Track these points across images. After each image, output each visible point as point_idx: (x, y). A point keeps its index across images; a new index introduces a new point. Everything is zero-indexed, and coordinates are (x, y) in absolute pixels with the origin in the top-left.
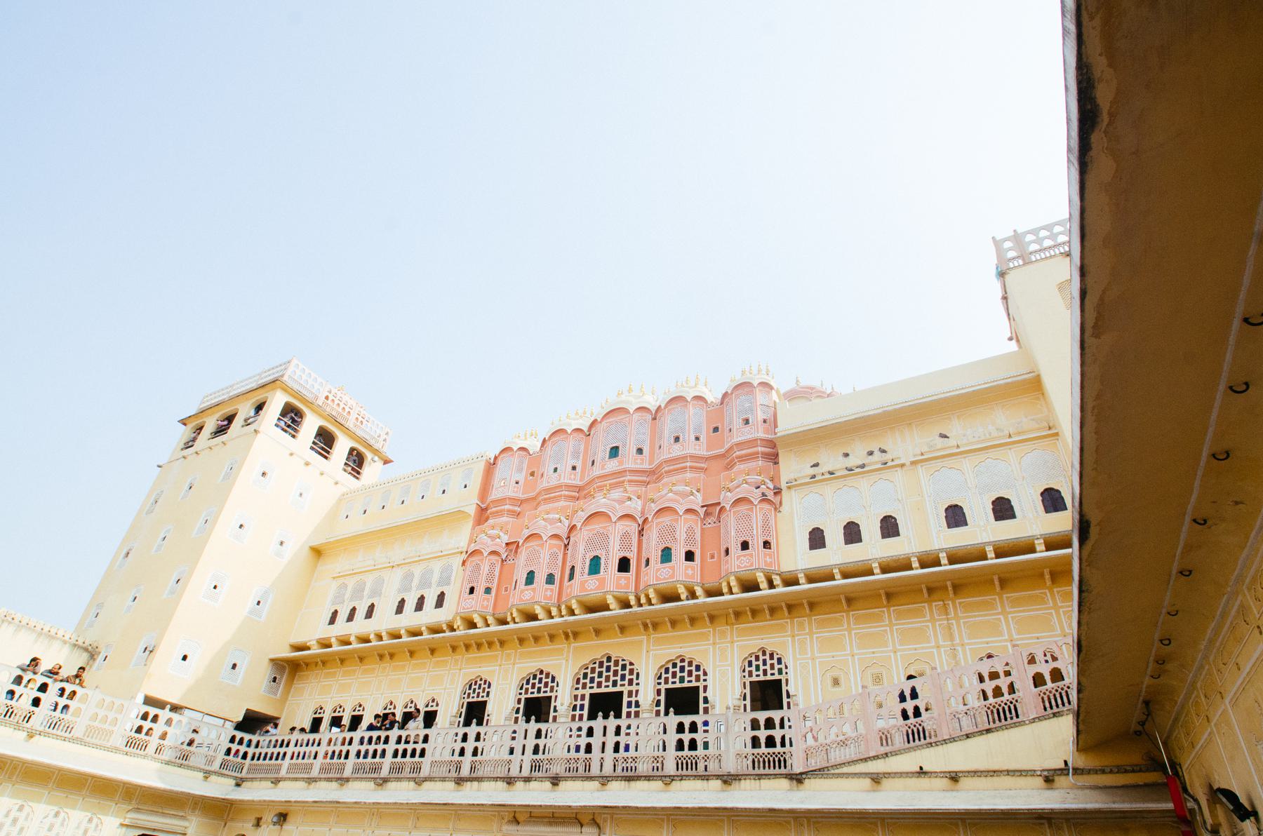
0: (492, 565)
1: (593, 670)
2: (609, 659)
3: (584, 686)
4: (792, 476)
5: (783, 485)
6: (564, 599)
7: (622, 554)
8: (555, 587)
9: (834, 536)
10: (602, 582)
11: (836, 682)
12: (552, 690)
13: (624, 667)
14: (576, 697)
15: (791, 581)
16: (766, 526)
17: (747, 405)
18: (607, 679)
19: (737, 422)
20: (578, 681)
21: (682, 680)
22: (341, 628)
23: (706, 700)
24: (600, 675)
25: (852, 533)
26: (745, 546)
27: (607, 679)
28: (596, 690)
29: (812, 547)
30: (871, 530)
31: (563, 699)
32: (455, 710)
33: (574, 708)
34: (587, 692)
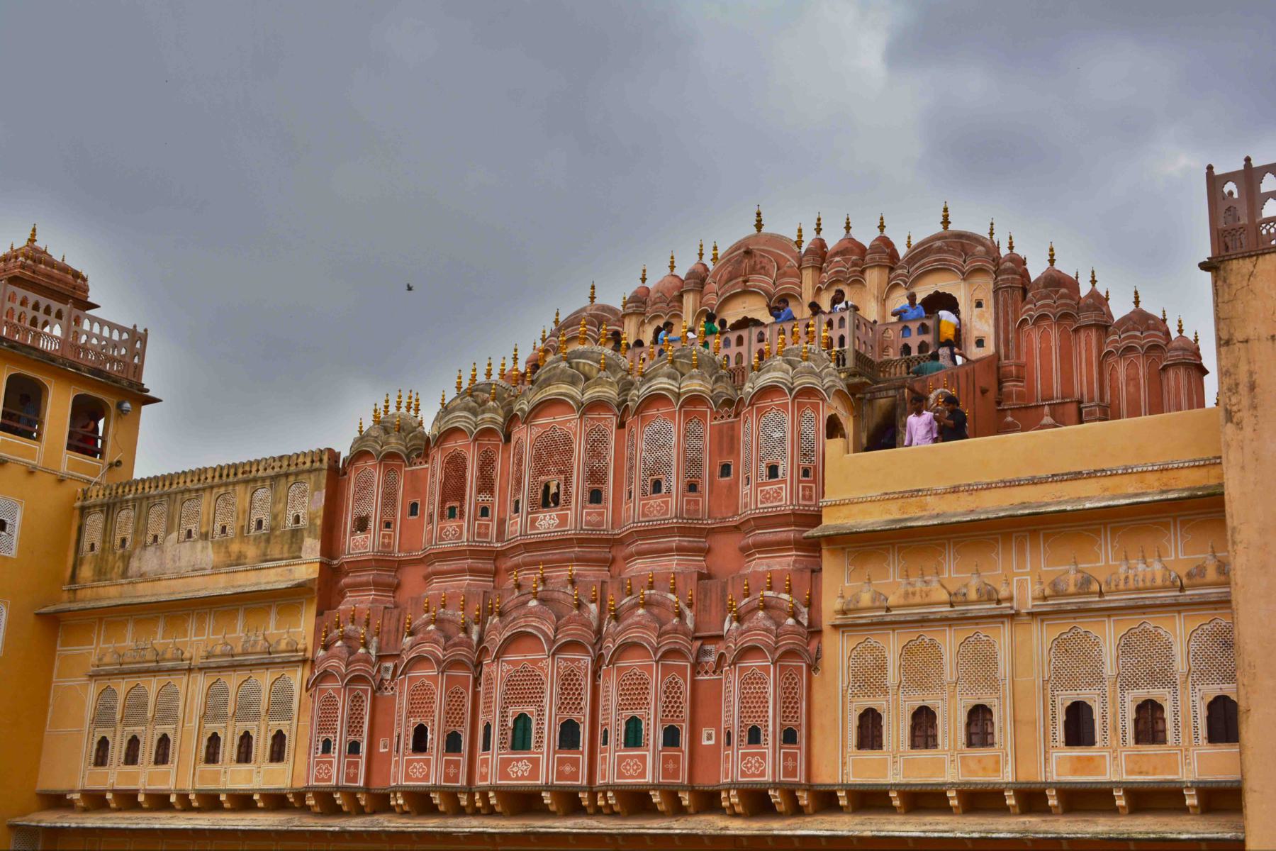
0: (357, 699)
4: (838, 604)
7: (566, 716)
8: (463, 760)
9: (896, 729)
10: (535, 762)
15: (826, 801)
16: (788, 703)
17: (776, 435)
26: (754, 736)
29: (861, 745)
30: (952, 725)
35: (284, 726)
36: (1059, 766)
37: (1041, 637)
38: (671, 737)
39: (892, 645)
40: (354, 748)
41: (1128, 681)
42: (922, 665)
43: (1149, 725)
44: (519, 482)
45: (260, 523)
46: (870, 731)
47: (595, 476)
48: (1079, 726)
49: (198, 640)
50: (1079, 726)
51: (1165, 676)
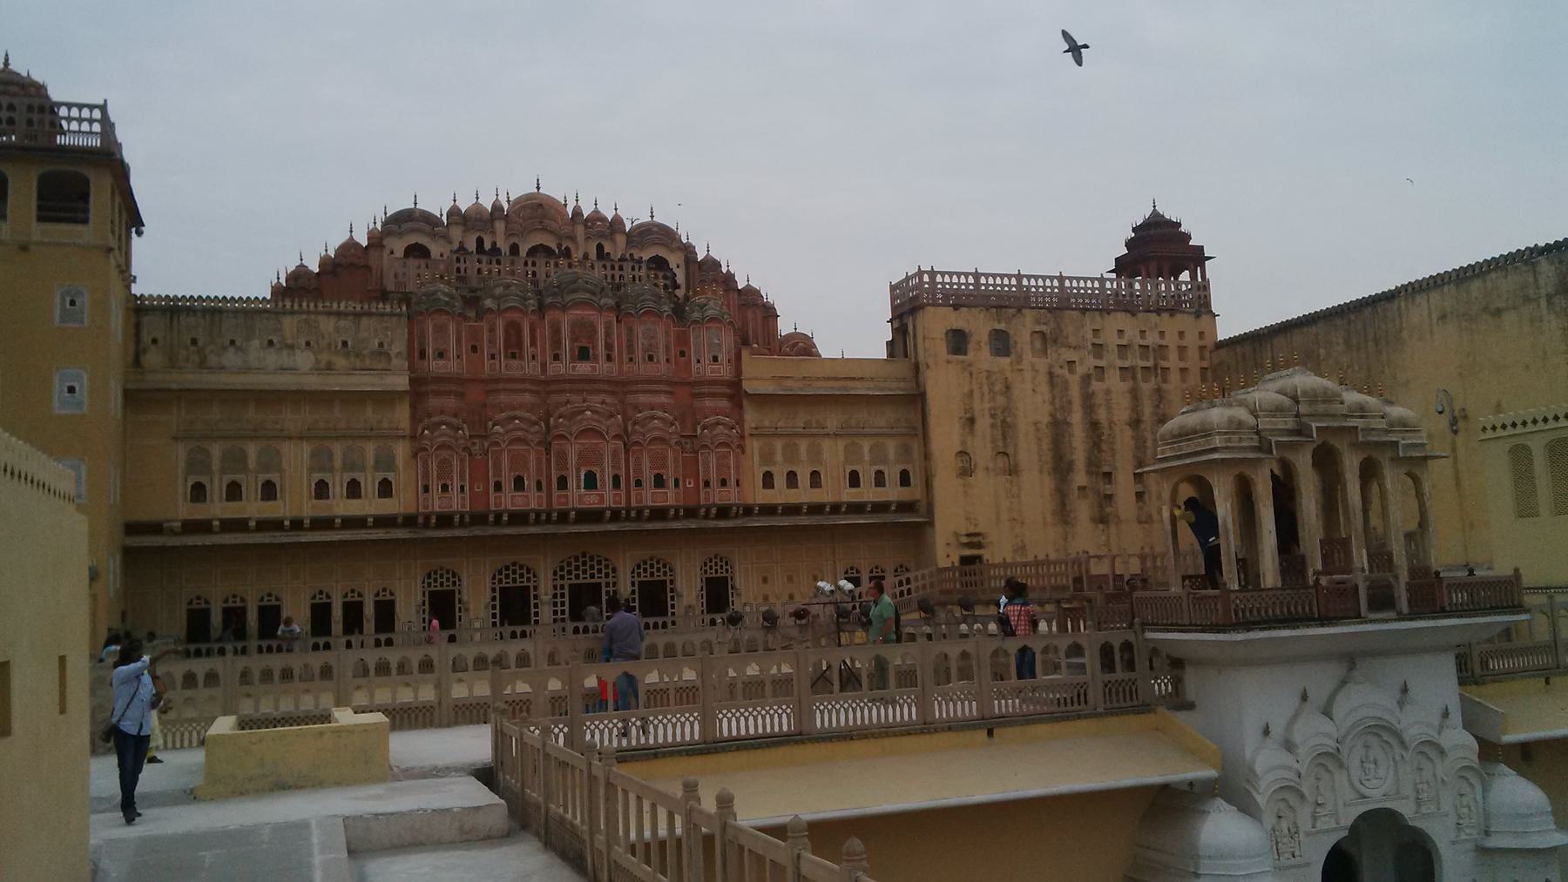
0: (462, 460)
1: (569, 564)
2: (584, 555)
3: (562, 577)
5: (747, 432)
6: (555, 506)
8: (544, 494)
9: (780, 481)
11: (765, 580)
12: (529, 580)
13: (599, 563)
14: (555, 587)
15: (748, 511)
16: (737, 468)
18: (585, 572)
19: (708, 358)
20: (555, 573)
21: (652, 574)
22: (217, 508)
23: (672, 590)
24: (577, 568)
25: (792, 478)
26: (724, 483)
27: (585, 572)
28: (575, 581)
31: (545, 588)
32: (420, 598)
33: (555, 596)
34: (566, 583)
35: (391, 476)
36: (848, 495)
37: (841, 444)
38: (677, 485)
39: (779, 445)
40: (462, 488)
41: (873, 463)
42: (791, 454)
43: (880, 479)
44: (557, 342)
45: (345, 344)
46: (768, 481)
47: (609, 347)
48: (854, 480)
49: (291, 419)
50: (854, 480)
51: (885, 461)
